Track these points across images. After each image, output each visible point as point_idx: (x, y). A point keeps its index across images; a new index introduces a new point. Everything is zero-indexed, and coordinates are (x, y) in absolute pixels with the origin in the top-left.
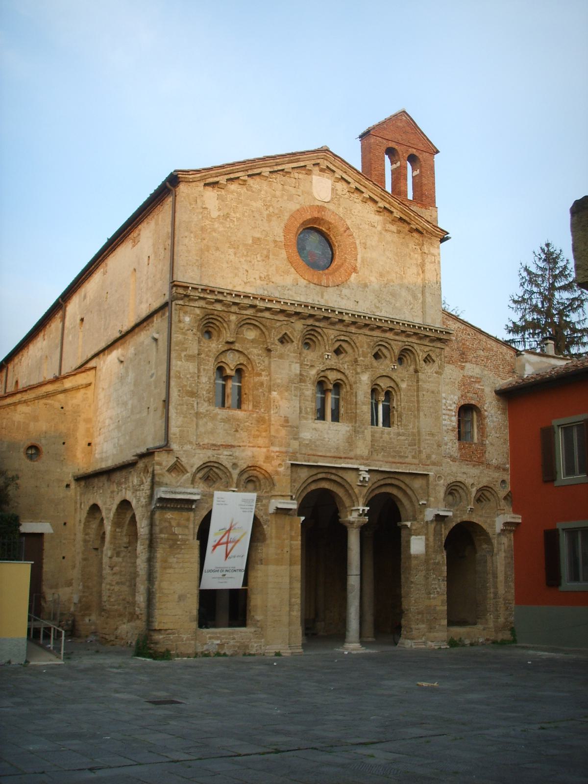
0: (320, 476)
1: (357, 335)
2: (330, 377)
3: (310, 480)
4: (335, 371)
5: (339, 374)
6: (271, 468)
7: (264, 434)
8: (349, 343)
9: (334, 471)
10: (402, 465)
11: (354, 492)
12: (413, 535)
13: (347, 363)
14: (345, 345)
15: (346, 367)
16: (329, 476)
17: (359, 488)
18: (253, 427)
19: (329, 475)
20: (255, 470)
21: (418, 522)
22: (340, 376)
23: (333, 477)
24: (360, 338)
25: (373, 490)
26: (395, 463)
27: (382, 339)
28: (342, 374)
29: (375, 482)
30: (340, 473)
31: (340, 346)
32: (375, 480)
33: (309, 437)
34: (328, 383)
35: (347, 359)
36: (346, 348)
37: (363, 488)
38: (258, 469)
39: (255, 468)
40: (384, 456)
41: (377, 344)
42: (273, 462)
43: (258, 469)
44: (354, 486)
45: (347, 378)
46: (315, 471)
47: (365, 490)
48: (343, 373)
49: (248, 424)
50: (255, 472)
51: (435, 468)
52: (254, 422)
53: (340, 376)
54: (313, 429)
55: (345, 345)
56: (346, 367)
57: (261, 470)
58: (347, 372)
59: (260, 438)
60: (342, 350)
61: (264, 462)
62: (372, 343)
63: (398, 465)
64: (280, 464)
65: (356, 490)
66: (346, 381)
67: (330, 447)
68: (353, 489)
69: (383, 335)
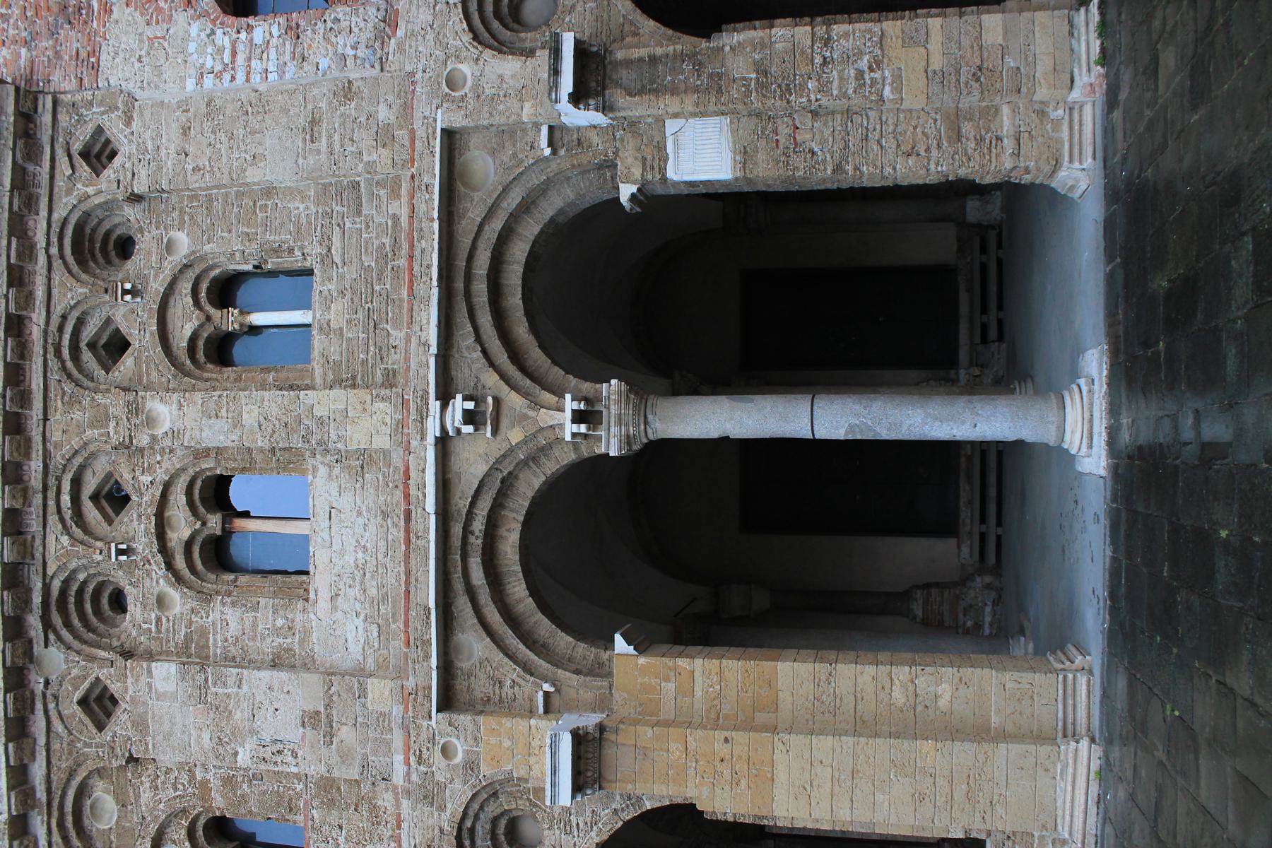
0: (478, 576)
1: (50, 447)
2: (186, 534)
3: (494, 616)
4: (167, 514)
5: (172, 498)
6: (458, 785)
7: (366, 788)
8: (82, 468)
9: (457, 530)
10: (417, 252)
11: (518, 444)
12: (662, 171)
13: (137, 474)
14: (90, 484)
15: (146, 479)
16: (476, 542)
17: (505, 422)
18: (349, 820)
19: (472, 539)
20: (472, 830)
21: (616, 153)
22: (178, 497)
23: (478, 525)
24: (56, 437)
25: (516, 356)
26: (411, 281)
27: (51, 349)
28: (173, 488)
29: (485, 352)
30: (461, 503)
31: (95, 498)
32: (478, 354)
33: (359, 622)
34: (206, 532)
35: (127, 476)
36: (101, 475)
37: (505, 410)
38: (468, 824)
39: (465, 834)
40: (397, 323)
41: (69, 364)
42: (439, 777)
43: (468, 824)
44: (497, 448)
45: (183, 470)
46: (462, 604)
47: (514, 400)
48: (167, 487)
49: (341, 840)
50: (479, 831)
51: (422, 108)
52: (334, 818)
53: (178, 497)
54: (334, 608)
55: (90, 486)
56: (146, 479)
57: (471, 813)
58: (161, 476)
59: (380, 803)
60: (106, 489)
61: (442, 808)
62: (68, 387)
63: (416, 268)
64: (446, 751)
65: (515, 436)
66: (191, 472)
67: (382, 543)
68: (512, 450)
69: (38, 349)
